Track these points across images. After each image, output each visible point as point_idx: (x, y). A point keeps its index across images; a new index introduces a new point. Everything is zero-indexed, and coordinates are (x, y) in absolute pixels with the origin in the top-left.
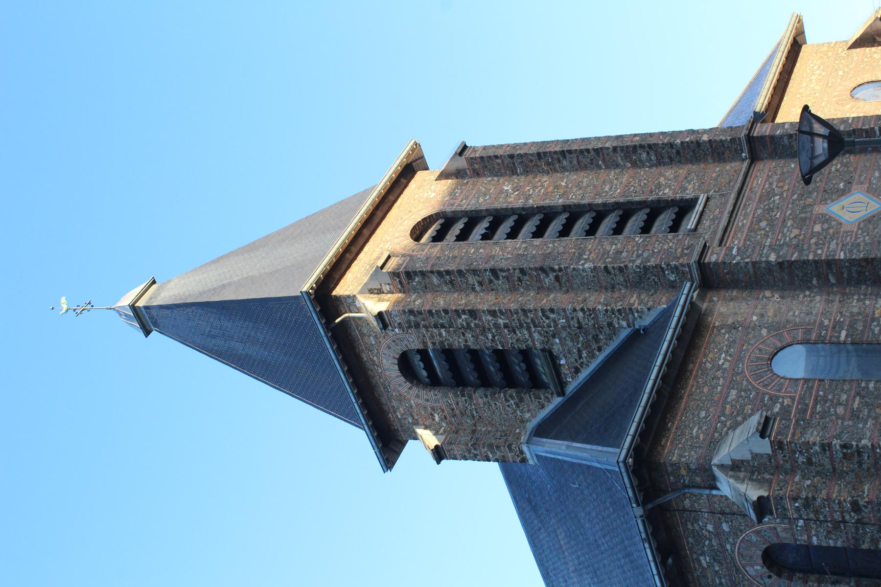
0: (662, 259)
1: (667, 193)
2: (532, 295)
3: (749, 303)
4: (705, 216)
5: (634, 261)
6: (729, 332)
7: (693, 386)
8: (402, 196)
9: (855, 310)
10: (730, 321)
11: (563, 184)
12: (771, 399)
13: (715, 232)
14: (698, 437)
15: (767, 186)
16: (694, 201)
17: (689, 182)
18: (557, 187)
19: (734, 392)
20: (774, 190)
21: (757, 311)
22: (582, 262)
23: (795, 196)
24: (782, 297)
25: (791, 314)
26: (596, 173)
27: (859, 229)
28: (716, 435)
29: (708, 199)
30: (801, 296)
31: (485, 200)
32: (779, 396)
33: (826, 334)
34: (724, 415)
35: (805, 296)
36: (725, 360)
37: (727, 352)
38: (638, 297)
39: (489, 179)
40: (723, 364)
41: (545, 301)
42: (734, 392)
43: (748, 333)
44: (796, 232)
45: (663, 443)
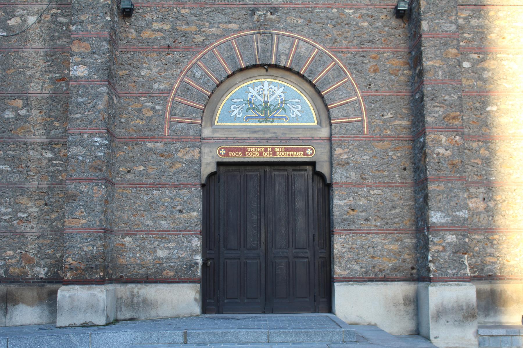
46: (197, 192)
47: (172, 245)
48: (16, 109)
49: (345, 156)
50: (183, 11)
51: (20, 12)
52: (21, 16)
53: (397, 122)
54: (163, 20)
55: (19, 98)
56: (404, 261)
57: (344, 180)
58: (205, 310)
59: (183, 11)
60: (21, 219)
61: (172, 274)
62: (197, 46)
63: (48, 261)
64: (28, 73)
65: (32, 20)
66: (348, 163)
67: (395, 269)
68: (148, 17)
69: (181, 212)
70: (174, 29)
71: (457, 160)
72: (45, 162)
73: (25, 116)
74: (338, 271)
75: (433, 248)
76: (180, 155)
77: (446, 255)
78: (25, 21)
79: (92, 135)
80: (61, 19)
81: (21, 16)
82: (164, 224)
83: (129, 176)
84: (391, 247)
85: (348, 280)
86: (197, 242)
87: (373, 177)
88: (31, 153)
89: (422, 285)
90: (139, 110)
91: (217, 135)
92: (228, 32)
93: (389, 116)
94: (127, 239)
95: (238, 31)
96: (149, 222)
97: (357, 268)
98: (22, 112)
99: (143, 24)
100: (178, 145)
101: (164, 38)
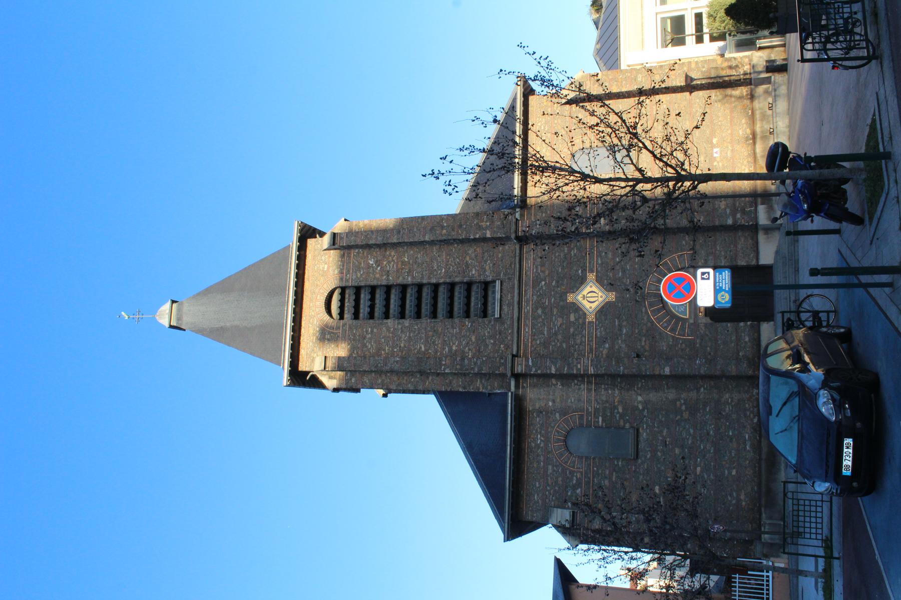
0: (490, 368)
1: (473, 273)
2: (418, 376)
3: (545, 389)
4: (503, 303)
5: (472, 369)
6: (538, 416)
7: (527, 461)
8: (306, 267)
9: (604, 398)
10: (537, 406)
11: (406, 260)
12: (570, 473)
13: (513, 318)
14: (538, 502)
15: (535, 271)
16: (494, 282)
17: (486, 262)
18: (403, 263)
19: (550, 467)
20: (539, 274)
21: (551, 397)
22: (443, 367)
23: (554, 284)
24: (562, 385)
25: (569, 401)
26: (424, 248)
27: (596, 319)
28: (547, 500)
29: (501, 282)
30: (573, 384)
31: (361, 275)
32: (574, 471)
33: (591, 418)
34: (548, 485)
35: (575, 384)
36: (541, 440)
37: (540, 433)
38: (481, 382)
39: (357, 251)
40: (540, 443)
41: (427, 384)
42: (550, 467)
43: (549, 417)
44: (560, 320)
45: (521, 506)
46: (718, 325)
47: (743, 335)
48: (681, 405)
49: (702, 261)
50: (637, 332)
51: (636, 404)
52: (638, 403)
53: (687, 239)
54: (640, 340)
55: (676, 403)
56: (748, 235)
57: (713, 261)
58: (773, 320)
59: (637, 332)
60: (732, 401)
61: (756, 334)
62: (652, 325)
63: (751, 389)
64: (664, 400)
65: (640, 398)
66: (706, 260)
67: (752, 239)
68: (639, 347)
69: (728, 331)
70: (644, 336)
71: (706, 214)
72: (705, 391)
73: (684, 400)
74: (754, 263)
75: (743, 223)
76: (702, 332)
77: (746, 217)
78: (640, 402)
79: (696, 364)
80: (640, 386)
81: (638, 403)
82: (734, 338)
83: (712, 354)
84: (742, 240)
85: (758, 259)
86: (742, 324)
87: (712, 248)
88: (701, 397)
89: (759, 227)
90: (682, 350)
91: (693, 317)
92: (647, 312)
93: (684, 242)
94: (740, 354)
95: (646, 308)
96: (733, 344)
97: (752, 255)
98: (682, 402)
99: (642, 349)
100: (698, 333)
101: (649, 340)
